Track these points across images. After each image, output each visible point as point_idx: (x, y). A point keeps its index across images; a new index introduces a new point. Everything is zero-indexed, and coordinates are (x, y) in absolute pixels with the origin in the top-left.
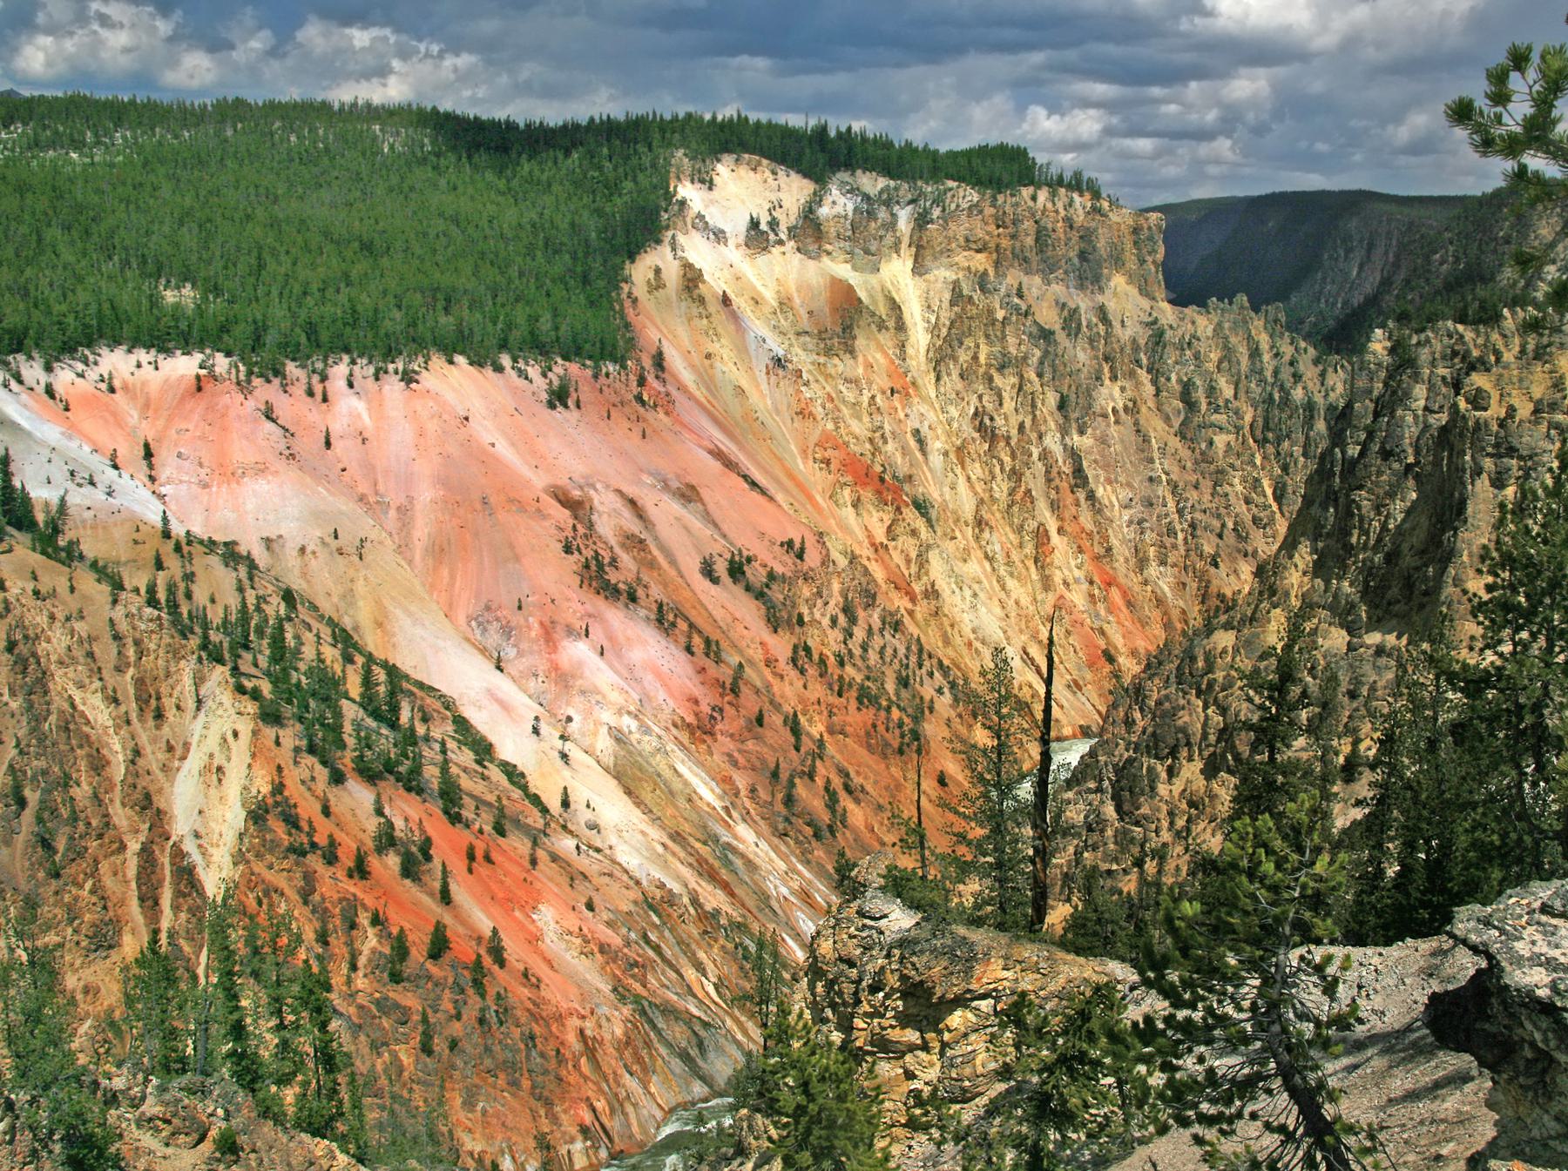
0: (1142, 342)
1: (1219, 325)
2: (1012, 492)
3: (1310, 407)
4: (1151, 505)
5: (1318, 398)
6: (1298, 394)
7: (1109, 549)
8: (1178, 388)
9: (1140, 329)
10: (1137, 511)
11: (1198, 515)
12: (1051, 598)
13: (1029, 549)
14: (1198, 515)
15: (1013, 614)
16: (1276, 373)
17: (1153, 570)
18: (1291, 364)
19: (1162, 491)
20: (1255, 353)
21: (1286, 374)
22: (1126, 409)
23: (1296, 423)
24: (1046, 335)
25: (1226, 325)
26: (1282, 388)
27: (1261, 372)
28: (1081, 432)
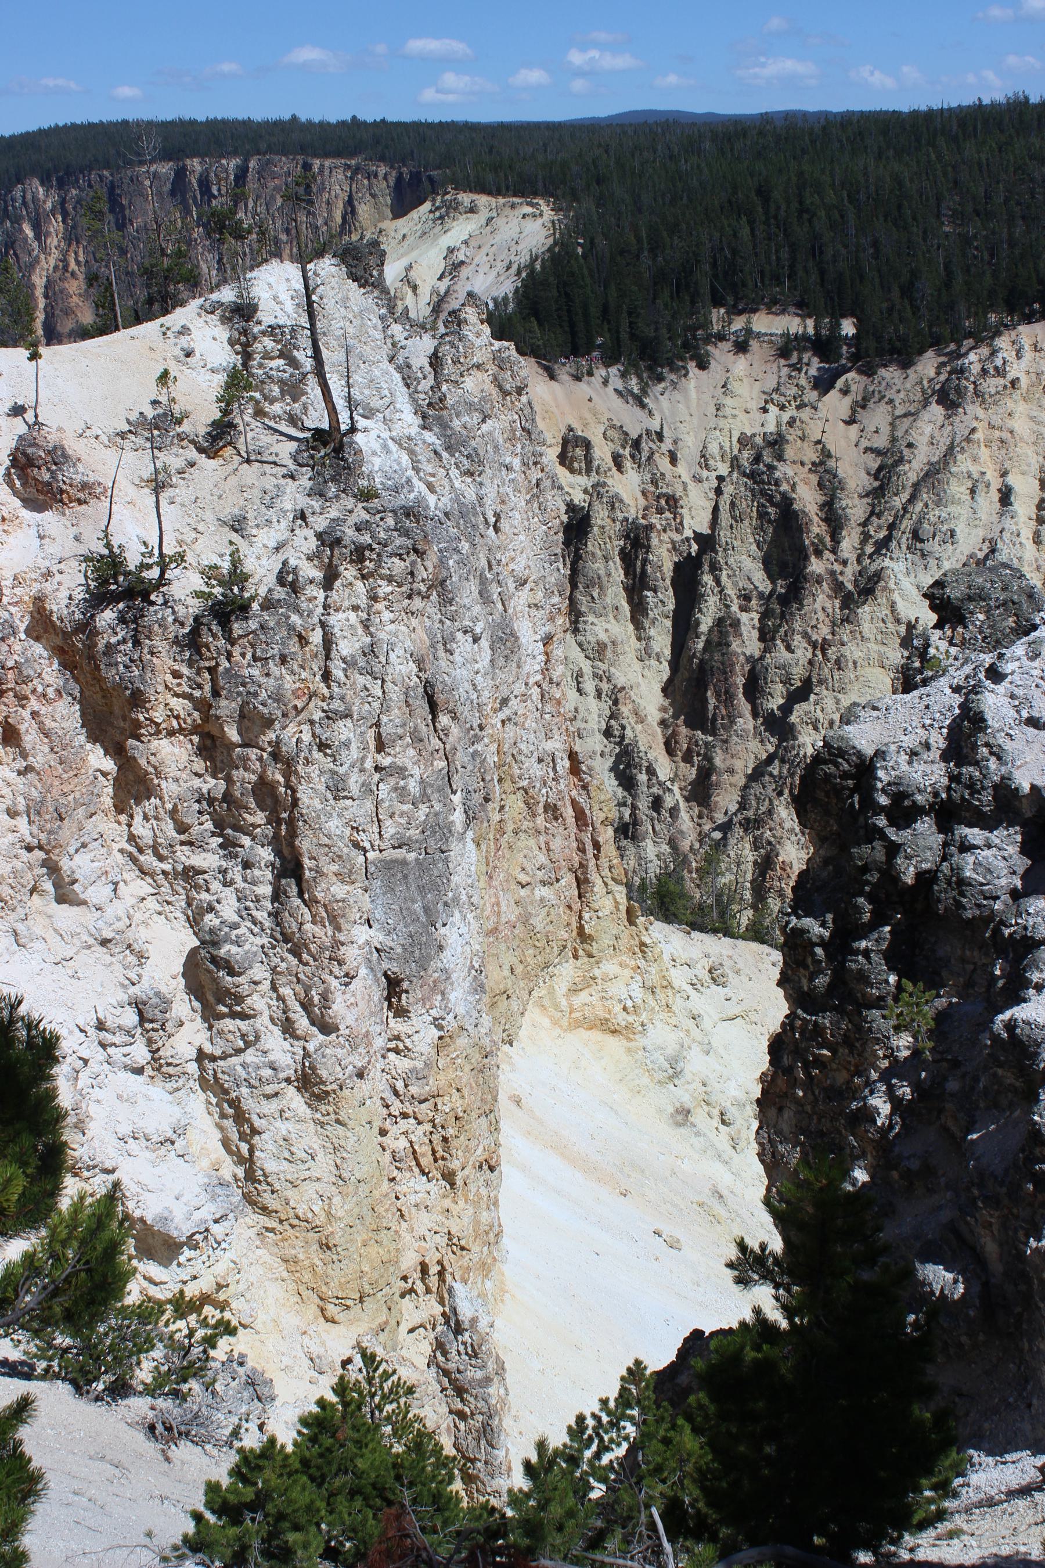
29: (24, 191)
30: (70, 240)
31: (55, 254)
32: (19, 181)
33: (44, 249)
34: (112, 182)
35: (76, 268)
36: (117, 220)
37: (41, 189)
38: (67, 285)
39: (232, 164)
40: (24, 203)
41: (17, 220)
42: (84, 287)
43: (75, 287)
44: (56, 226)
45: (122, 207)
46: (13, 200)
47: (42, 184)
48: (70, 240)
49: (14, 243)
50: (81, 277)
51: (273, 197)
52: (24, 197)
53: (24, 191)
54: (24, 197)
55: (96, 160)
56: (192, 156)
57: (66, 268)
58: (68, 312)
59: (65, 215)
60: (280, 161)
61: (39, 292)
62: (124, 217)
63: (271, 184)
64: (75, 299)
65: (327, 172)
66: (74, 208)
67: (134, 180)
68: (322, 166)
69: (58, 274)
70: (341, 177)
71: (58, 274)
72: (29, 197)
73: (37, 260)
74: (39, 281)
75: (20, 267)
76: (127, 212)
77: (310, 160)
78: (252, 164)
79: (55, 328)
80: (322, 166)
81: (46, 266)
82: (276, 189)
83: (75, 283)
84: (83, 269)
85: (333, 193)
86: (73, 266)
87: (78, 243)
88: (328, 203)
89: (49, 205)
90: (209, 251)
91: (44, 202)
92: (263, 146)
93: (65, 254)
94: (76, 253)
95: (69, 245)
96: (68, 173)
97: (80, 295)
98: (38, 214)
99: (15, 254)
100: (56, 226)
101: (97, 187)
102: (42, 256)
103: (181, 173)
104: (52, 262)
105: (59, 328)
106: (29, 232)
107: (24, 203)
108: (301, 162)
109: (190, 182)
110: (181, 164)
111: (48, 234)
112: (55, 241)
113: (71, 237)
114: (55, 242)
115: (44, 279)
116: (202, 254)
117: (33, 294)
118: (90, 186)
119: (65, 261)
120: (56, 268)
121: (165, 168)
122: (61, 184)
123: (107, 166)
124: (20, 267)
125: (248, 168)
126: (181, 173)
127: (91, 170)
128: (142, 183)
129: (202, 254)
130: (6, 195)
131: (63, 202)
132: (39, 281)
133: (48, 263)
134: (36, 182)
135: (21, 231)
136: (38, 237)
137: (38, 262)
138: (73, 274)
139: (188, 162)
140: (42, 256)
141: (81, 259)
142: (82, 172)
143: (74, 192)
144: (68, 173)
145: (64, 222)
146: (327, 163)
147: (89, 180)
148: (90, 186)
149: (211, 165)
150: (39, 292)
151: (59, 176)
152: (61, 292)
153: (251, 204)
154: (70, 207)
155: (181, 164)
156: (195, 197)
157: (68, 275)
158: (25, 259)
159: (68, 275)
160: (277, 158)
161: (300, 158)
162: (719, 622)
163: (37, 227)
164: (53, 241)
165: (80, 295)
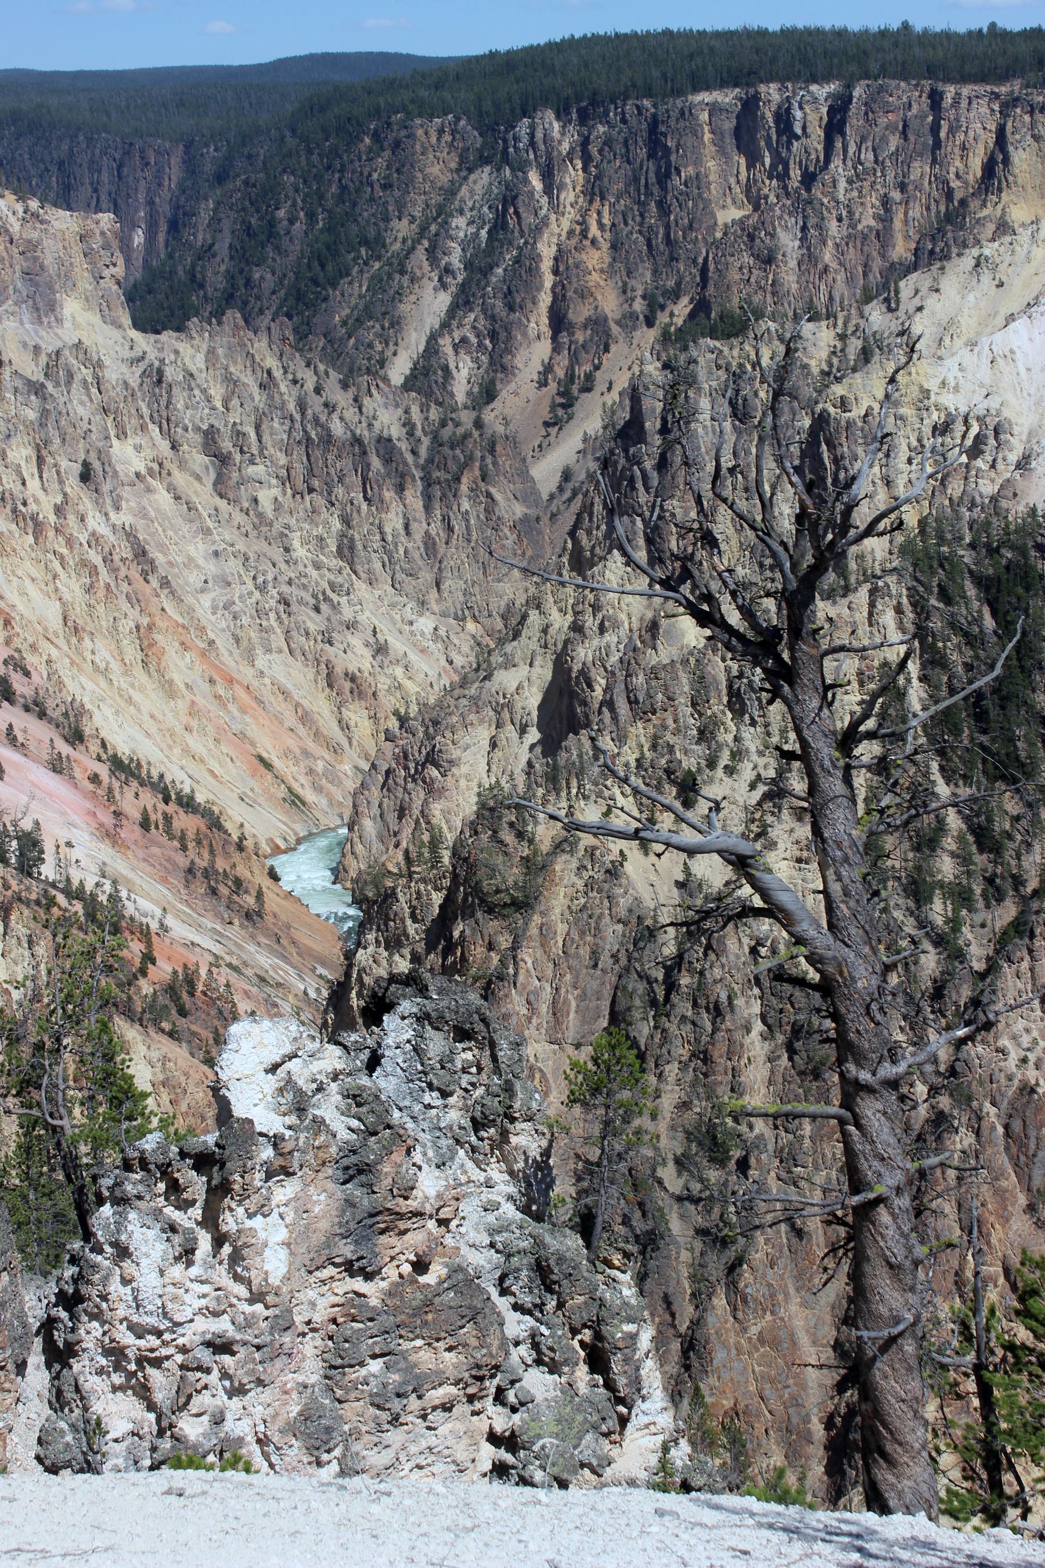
0: (134, 382)
1: (211, 352)
2: (89, 590)
3: (357, 441)
4: (229, 584)
5: (362, 431)
6: (337, 428)
7: (212, 643)
8: (199, 439)
9: (124, 368)
10: (216, 593)
11: (286, 589)
12: (182, 705)
13: (132, 653)
14: (286, 589)
15: (153, 730)
16: (302, 406)
17: (261, 661)
18: (318, 390)
19: (234, 566)
20: (267, 384)
21: (315, 404)
22: (150, 472)
23: (346, 464)
24: (37, 389)
25: (220, 351)
26: (316, 421)
27: (283, 406)
28: (118, 508)
29: (532, 127)
30: (593, 194)
31: (571, 214)
32: (526, 112)
33: (555, 207)
34: (654, 116)
35: (598, 234)
36: (659, 167)
37: (556, 125)
38: (584, 257)
39: (822, 91)
40: (532, 143)
41: (520, 167)
42: (608, 260)
43: (595, 259)
44: (573, 176)
45: (667, 150)
46: (516, 139)
47: (558, 118)
48: (593, 194)
49: (516, 197)
50: (605, 246)
51: (884, 139)
52: (532, 135)
53: (532, 127)
54: (532, 135)
55: (634, 86)
56: (768, 80)
57: (584, 234)
58: (584, 294)
59: (587, 159)
60: (898, 87)
61: (546, 265)
62: (669, 164)
63: (883, 121)
64: (595, 276)
65: (964, 104)
66: (601, 151)
67: (686, 114)
68: (958, 94)
69: (573, 242)
70: (984, 110)
71: (573, 242)
72: (539, 135)
73: (545, 222)
74: (547, 251)
75: (522, 231)
76: (673, 157)
77: (940, 87)
78: (857, 92)
79: (565, 316)
80: (958, 94)
81: (557, 231)
82: (890, 127)
83: (596, 255)
84: (608, 235)
85: (971, 134)
86: (594, 230)
87: (603, 198)
88: (963, 148)
89: (565, 147)
90: (790, 214)
91: (560, 142)
92: (874, 67)
93: (584, 214)
94: (599, 213)
95: (591, 202)
96: (594, 103)
97: (602, 271)
98: (550, 158)
99: (517, 213)
100: (573, 176)
101: (633, 122)
102: (553, 217)
103: (750, 106)
104: (566, 225)
105: (571, 315)
106: (536, 182)
107: (532, 143)
108: (927, 89)
109: (763, 117)
110: (752, 91)
111: (561, 187)
112: (572, 194)
113: (594, 191)
114: (571, 197)
115: (554, 248)
116: (781, 218)
117: (538, 268)
118: (624, 121)
119: (583, 223)
120: (571, 233)
121: (728, 97)
122: (584, 118)
123: (649, 94)
124: (522, 231)
125: (850, 98)
126: (750, 106)
127: (626, 98)
128: (697, 119)
129: (781, 218)
130: (507, 131)
131: (585, 143)
132: (547, 251)
133: (560, 226)
134: (550, 115)
135: (526, 181)
136: (548, 190)
137: (547, 225)
138: (594, 242)
139: (762, 88)
140: (553, 217)
141: (606, 221)
142: (613, 101)
143: (601, 129)
144: (594, 103)
145: (585, 169)
146: (966, 91)
147: (623, 113)
148: (624, 121)
149: (795, 94)
150: (546, 265)
151: (583, 106)
152: (577, 267)
153: (852, 149)
154: (594, 150)
155: (752, 91)
156: (769, 137)
157: (587, 243)
158: (529, 219)
159: (587, 243)
160: (893, 83)
161: (927, 84)
162: (977, 437)
163: (548, 176)
164: (568, 196)
165: (602, 271)
